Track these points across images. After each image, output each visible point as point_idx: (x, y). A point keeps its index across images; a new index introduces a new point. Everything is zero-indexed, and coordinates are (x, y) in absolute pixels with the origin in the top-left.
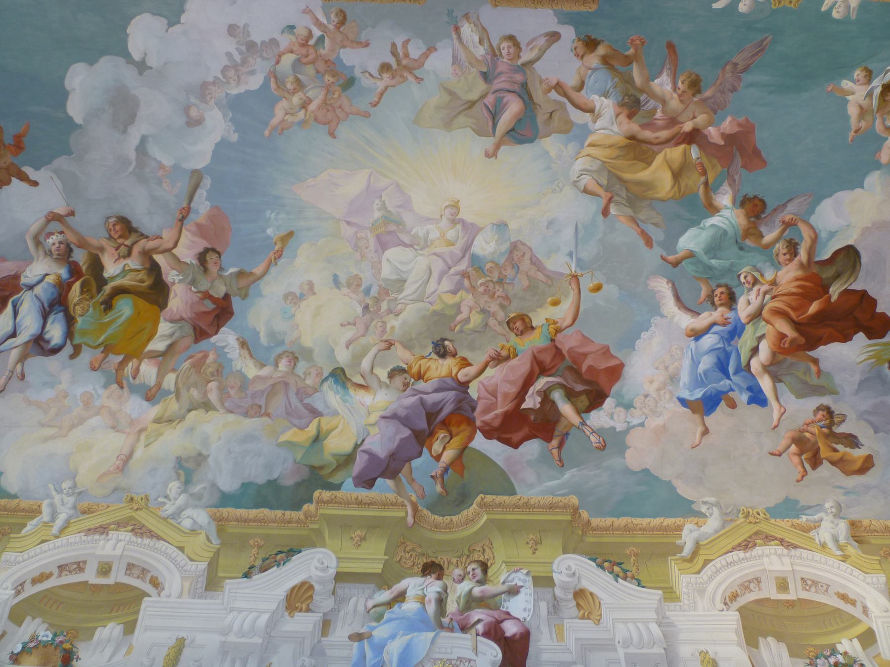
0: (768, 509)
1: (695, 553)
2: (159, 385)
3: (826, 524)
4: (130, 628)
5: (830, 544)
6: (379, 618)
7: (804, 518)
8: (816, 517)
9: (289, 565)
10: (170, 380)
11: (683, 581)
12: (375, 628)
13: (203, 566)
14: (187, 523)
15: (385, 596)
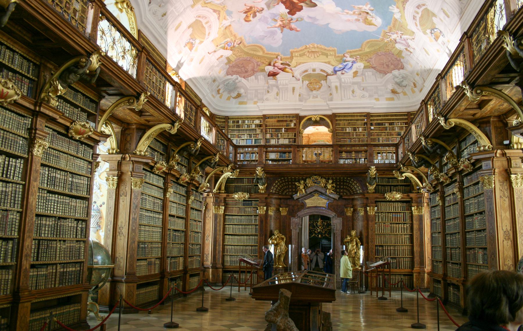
0: (227, 10)
1: (208, 3)
3: (228, 21)
5: (222, 25)
7: (228, 17)
8: (229, 19)
11: (199, 6)
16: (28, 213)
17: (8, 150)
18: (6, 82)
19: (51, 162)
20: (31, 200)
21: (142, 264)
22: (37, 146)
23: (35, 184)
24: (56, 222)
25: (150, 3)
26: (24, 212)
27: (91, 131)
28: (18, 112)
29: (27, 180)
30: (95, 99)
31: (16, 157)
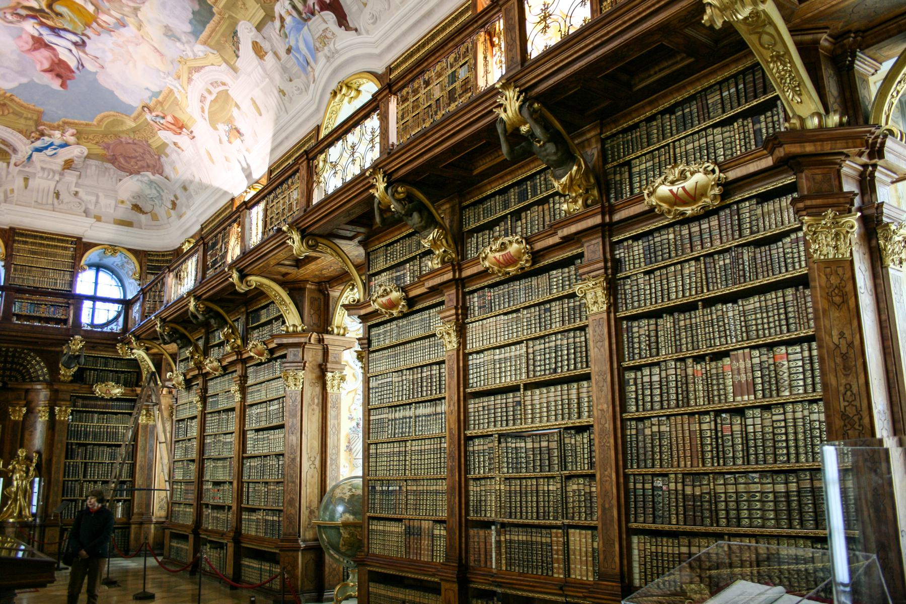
2: (117, 19)
4: (237, 106)
6: (286, 36)
9: (241, 39)
10: (113, 12)
12: (289, 42)
13: (224, 65)
14: (201, 54)
15: (277, 23)
21: (393, 529)
25: (356, 30)
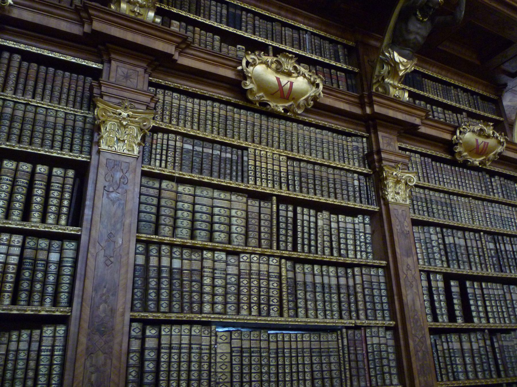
16: (409, 327)
17: (331, 201)
18: (278, 62)
19: (436, 215)
20: (409, 298)
22: (391, 184)
23: (410, 261)
24: (488, 342)
26: (400, 326)
27: (500, 143)
28: (334, 126)
29: (390, 255)
30: (488, 95)
31: (352, 212)
